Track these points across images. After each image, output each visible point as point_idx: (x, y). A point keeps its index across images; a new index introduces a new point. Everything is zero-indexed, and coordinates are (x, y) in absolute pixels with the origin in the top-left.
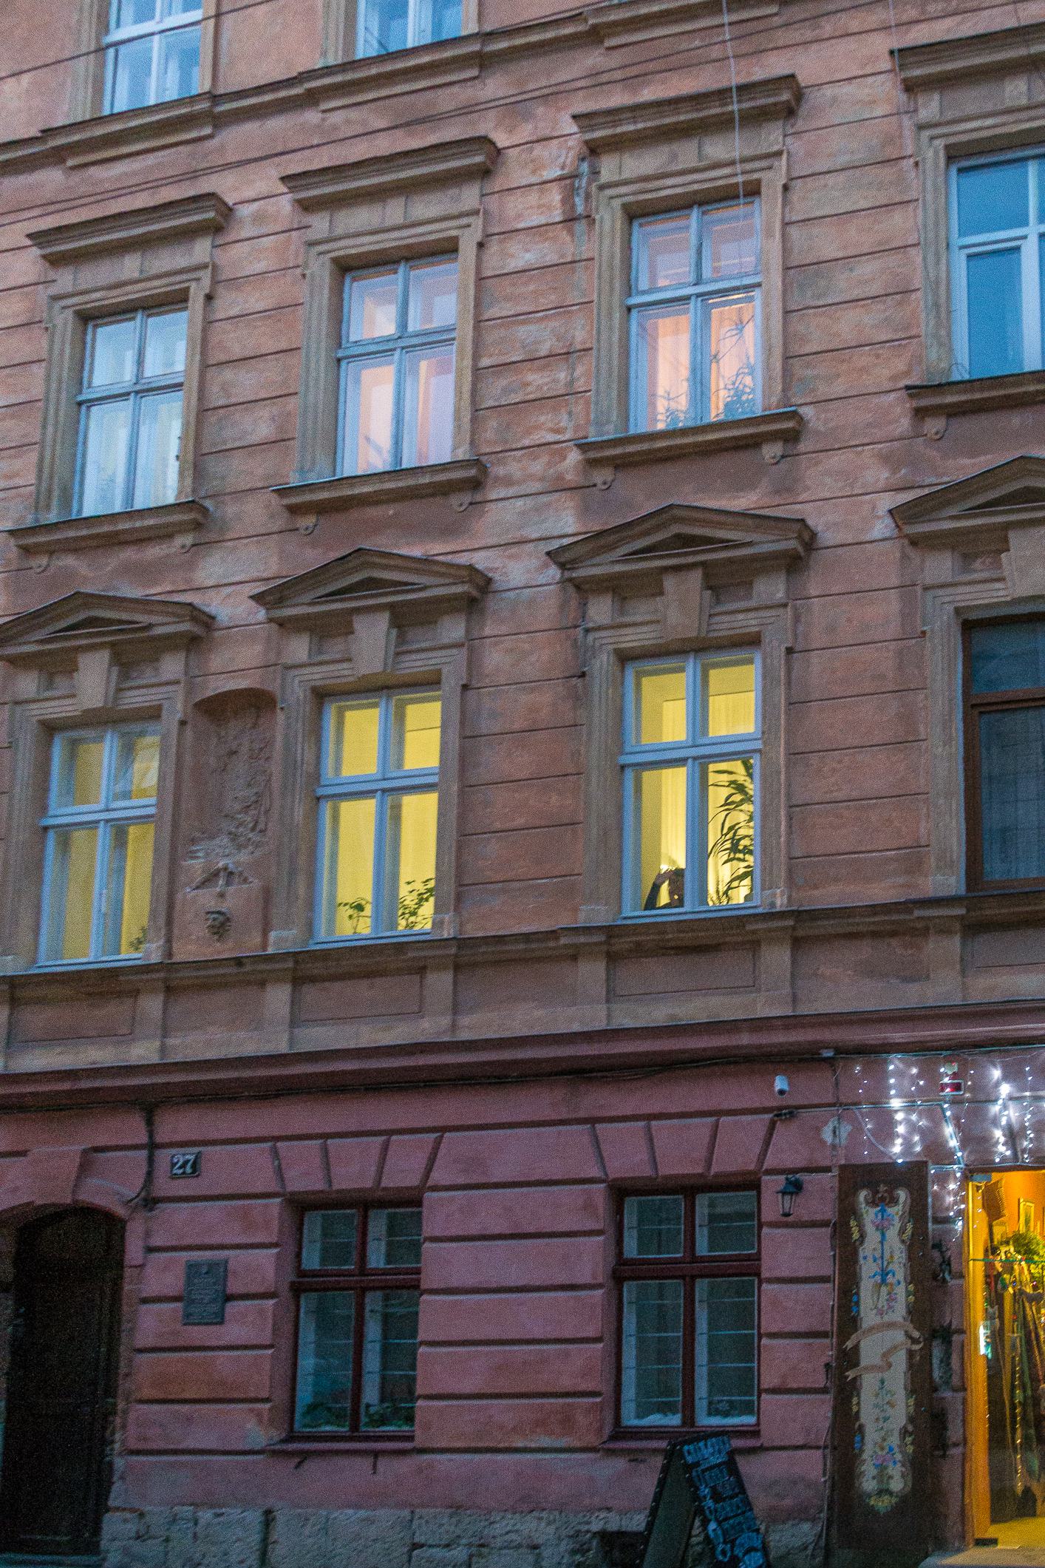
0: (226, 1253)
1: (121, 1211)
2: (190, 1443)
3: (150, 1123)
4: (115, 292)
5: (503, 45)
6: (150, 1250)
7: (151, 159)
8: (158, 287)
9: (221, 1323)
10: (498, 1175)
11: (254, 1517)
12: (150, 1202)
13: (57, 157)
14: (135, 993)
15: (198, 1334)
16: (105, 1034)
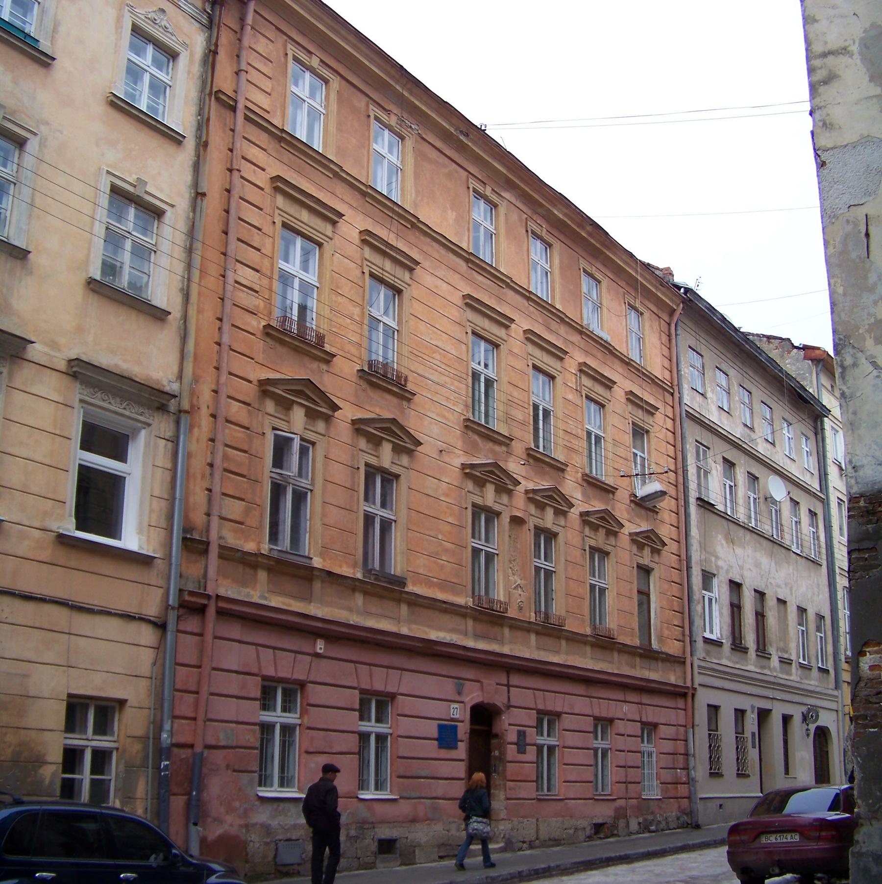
0: (525, 728)
1: (503, 708)
2: (521, 796)
3: (508, 677)
4: (483, 331)
5: (567, 320)
6: (510, 725)
7: (489, 282)
8: (493, 338)
9: (525, 754)
10: (576, 711)
11: (534, 820)
12: (509, 706)
13: (467, 261)
14: (502, 626)
15: (521, 757)
16: (495, 639)
